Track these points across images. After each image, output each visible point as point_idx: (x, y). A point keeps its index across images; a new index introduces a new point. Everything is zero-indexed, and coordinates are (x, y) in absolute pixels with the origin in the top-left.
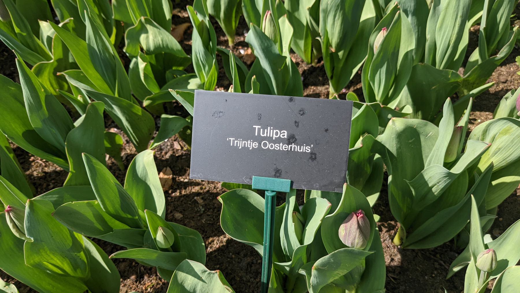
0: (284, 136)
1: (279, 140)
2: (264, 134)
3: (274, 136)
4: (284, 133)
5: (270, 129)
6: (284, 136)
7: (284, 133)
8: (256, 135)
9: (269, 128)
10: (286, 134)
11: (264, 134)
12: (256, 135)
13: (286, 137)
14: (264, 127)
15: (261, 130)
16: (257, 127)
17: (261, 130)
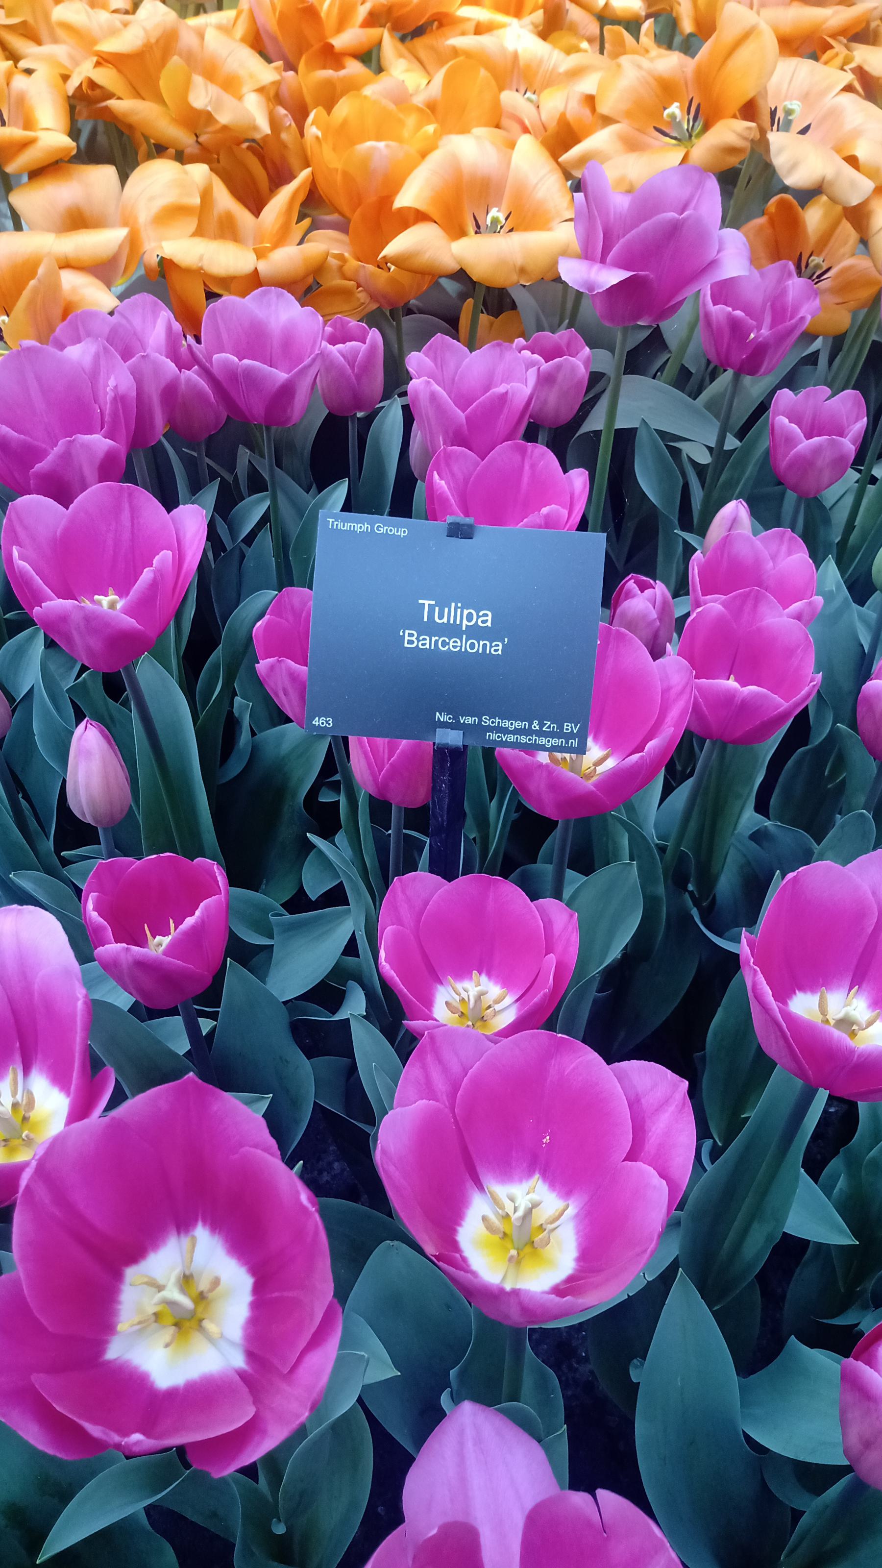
0: (487, 621)
1: (475, 632)
2: (441, 617)
3: (465, 622)
4: (487, 615)
5: (456, 608)
6: (487, 621)
7: (487, 615)
8: (425, 619)
9: (453, 605)
10: (489, 618)
11: (441, 617)
12: (425, 619)
14: (443, 604)
15: (437, 609)
16: (427, 603)
17: (437, 609)
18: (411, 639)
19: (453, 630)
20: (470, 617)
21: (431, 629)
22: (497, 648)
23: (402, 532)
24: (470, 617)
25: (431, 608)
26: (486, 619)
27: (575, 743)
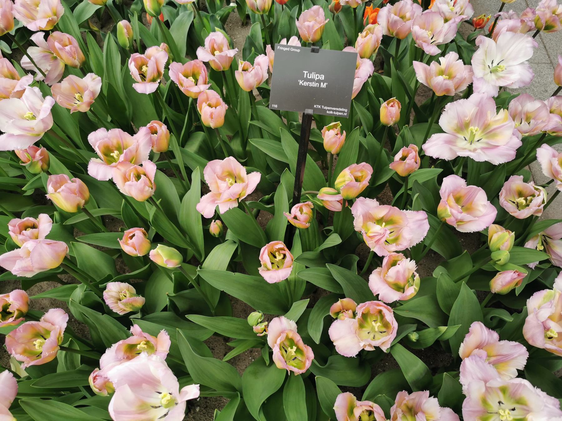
1: (319, 81)
14: (310, 72)
16: (306, 72)
19: (312, 80)
20: (318, 77)
24: (318, 77)
25: (307, 74)
26: (322, 77)
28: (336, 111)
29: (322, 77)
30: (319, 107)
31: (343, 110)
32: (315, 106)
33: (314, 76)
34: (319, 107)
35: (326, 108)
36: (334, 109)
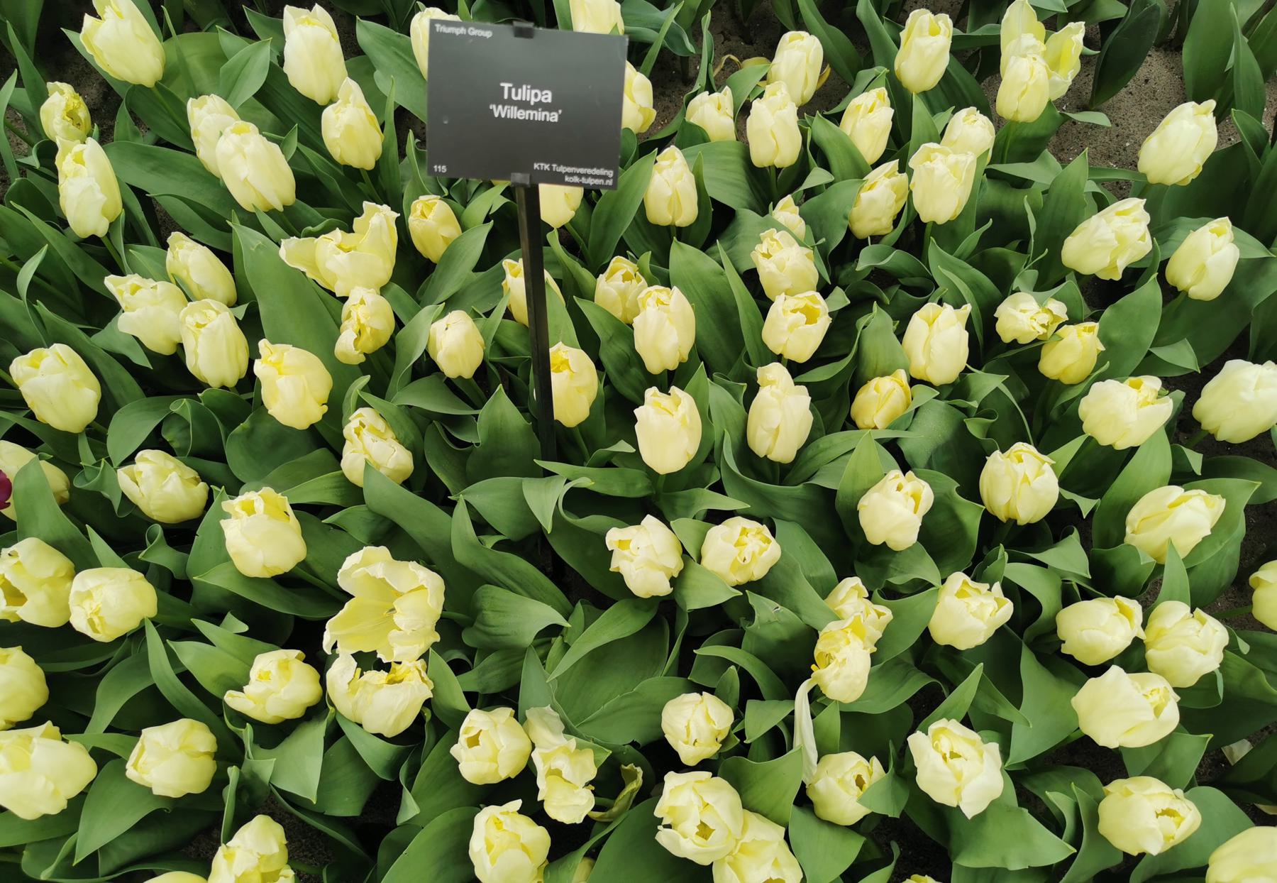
1: (540, 106)
8: (506, 97)
12: (506, 97)
13: (549, 100)
14: (518, 86)
15: (513, 90)
16: (506, 86)
17: (513, 90)
18: (498, 111)
19: (524, 105)
20: (536, 95)
21: (510, 102)
22: (554, 117)
23: (488, 34)
24: (536, 95)
25: (510, 89)
26: (547, 97)
27: (610, 182)
28: (587, 176)
29: (547, 97)
30: (547, 167)
31: (602, 172)
32: (536, 166)
33: (527, 93)
34: (547, 167)
35: (562, 169)
36: (582, 171)
